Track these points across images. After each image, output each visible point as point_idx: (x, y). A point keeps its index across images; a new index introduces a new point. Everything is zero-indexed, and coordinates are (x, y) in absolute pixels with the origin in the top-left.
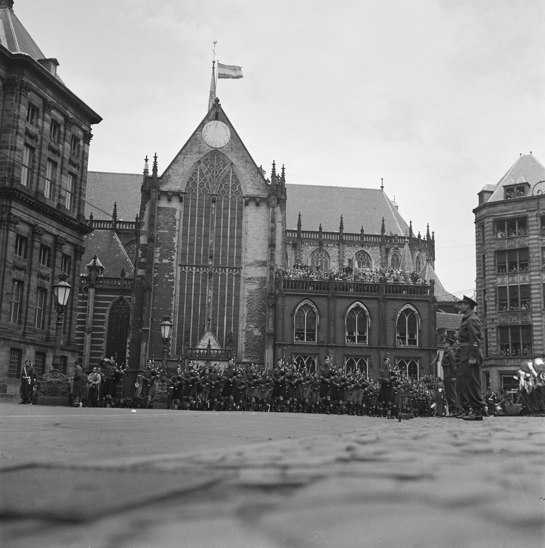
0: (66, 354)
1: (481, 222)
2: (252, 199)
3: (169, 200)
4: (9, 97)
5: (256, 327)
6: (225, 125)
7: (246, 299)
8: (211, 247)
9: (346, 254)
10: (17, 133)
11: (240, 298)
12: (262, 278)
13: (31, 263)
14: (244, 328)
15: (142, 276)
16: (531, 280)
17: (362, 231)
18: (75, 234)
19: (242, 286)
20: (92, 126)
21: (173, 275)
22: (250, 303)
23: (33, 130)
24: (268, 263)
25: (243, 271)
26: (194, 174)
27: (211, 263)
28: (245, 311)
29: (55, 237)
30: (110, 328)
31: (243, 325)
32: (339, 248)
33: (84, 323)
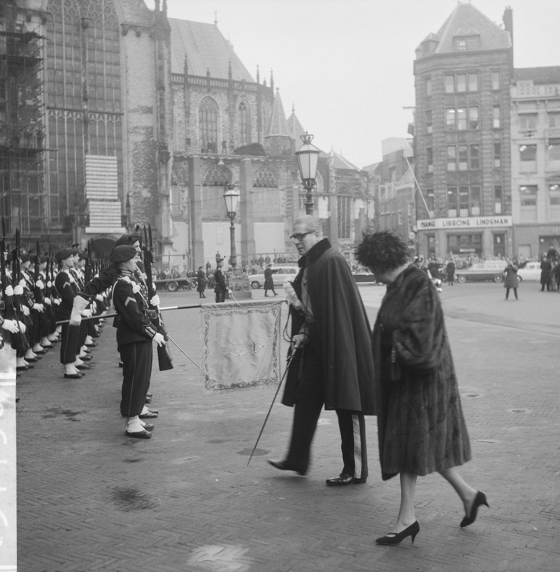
1: (428, 73)
2: (133, 27)
5: (145, 187)
7: (131, 153)
8: (85, 87)
9: (192, 99)
11: (123, 152)
12: (147, 128)
14: (131, 187)
16: (482, 140)
17: (208, 73)
19: (125, 137)
21: (41, 121)
25: (124, 118)
27: (85, 107)
28: (130, 167)
32: (184, 92)
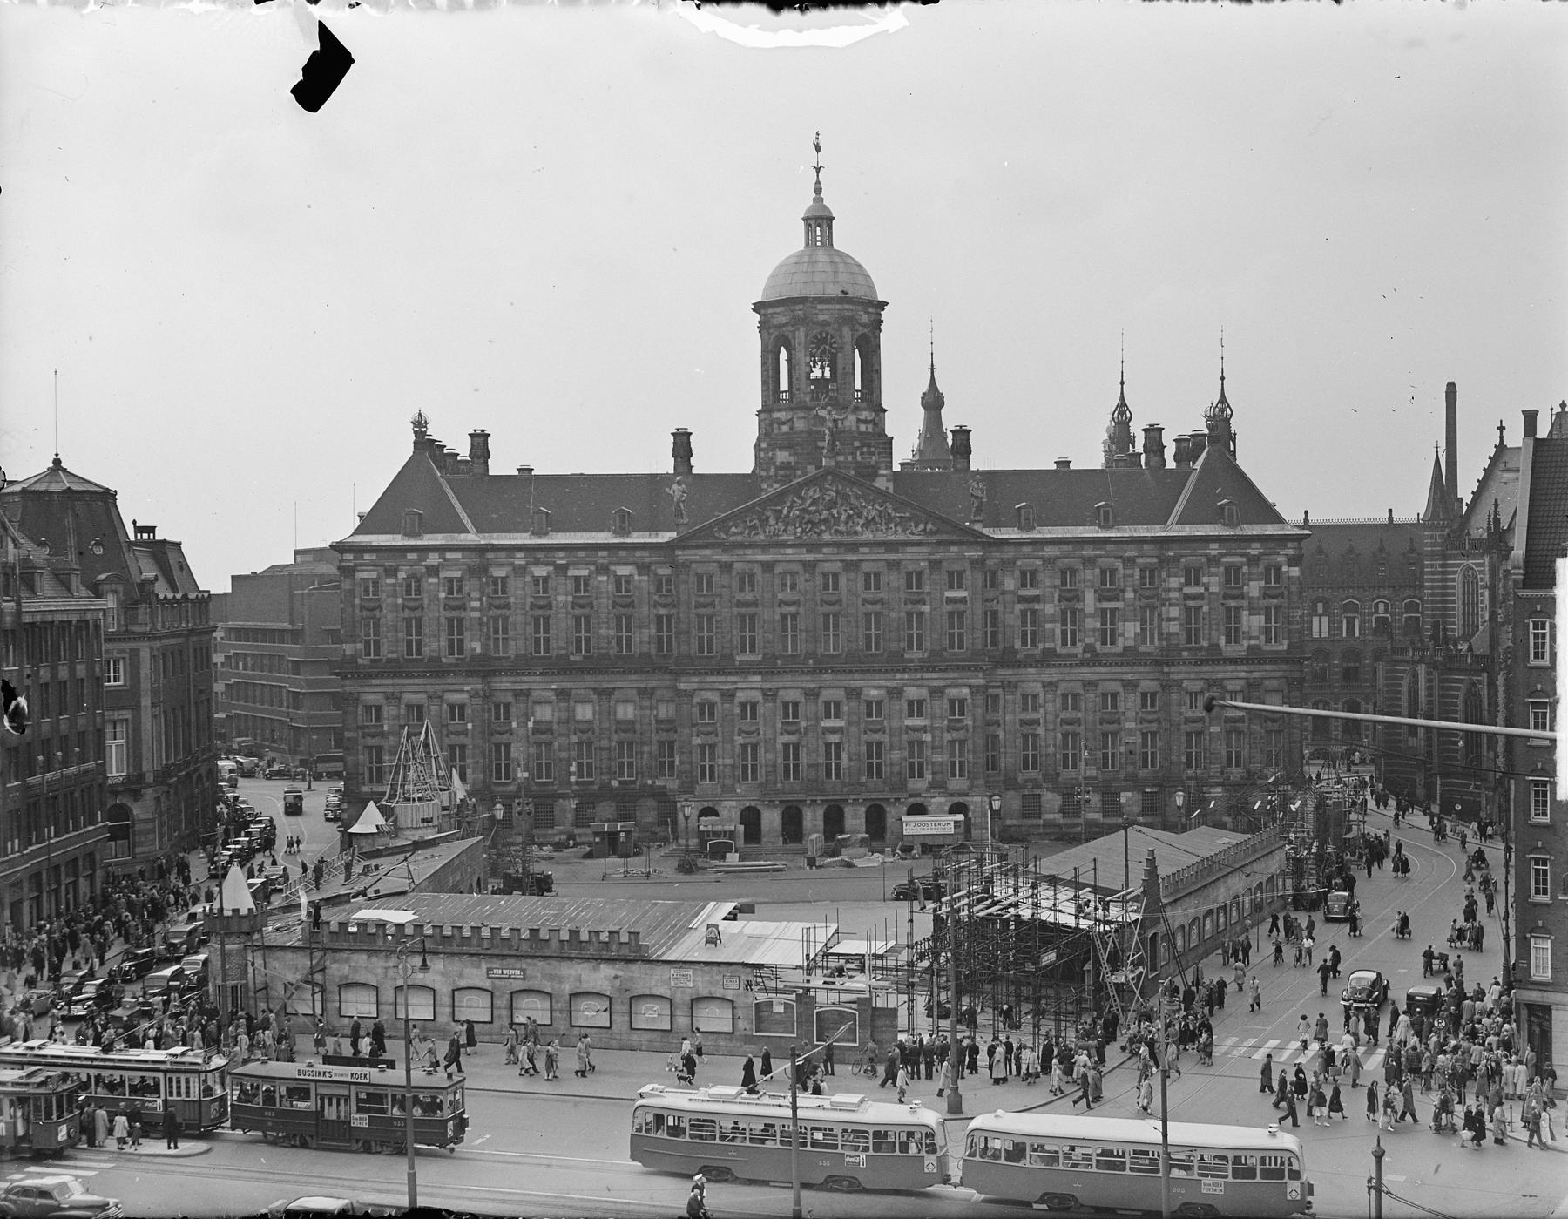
18: (1284, 667)
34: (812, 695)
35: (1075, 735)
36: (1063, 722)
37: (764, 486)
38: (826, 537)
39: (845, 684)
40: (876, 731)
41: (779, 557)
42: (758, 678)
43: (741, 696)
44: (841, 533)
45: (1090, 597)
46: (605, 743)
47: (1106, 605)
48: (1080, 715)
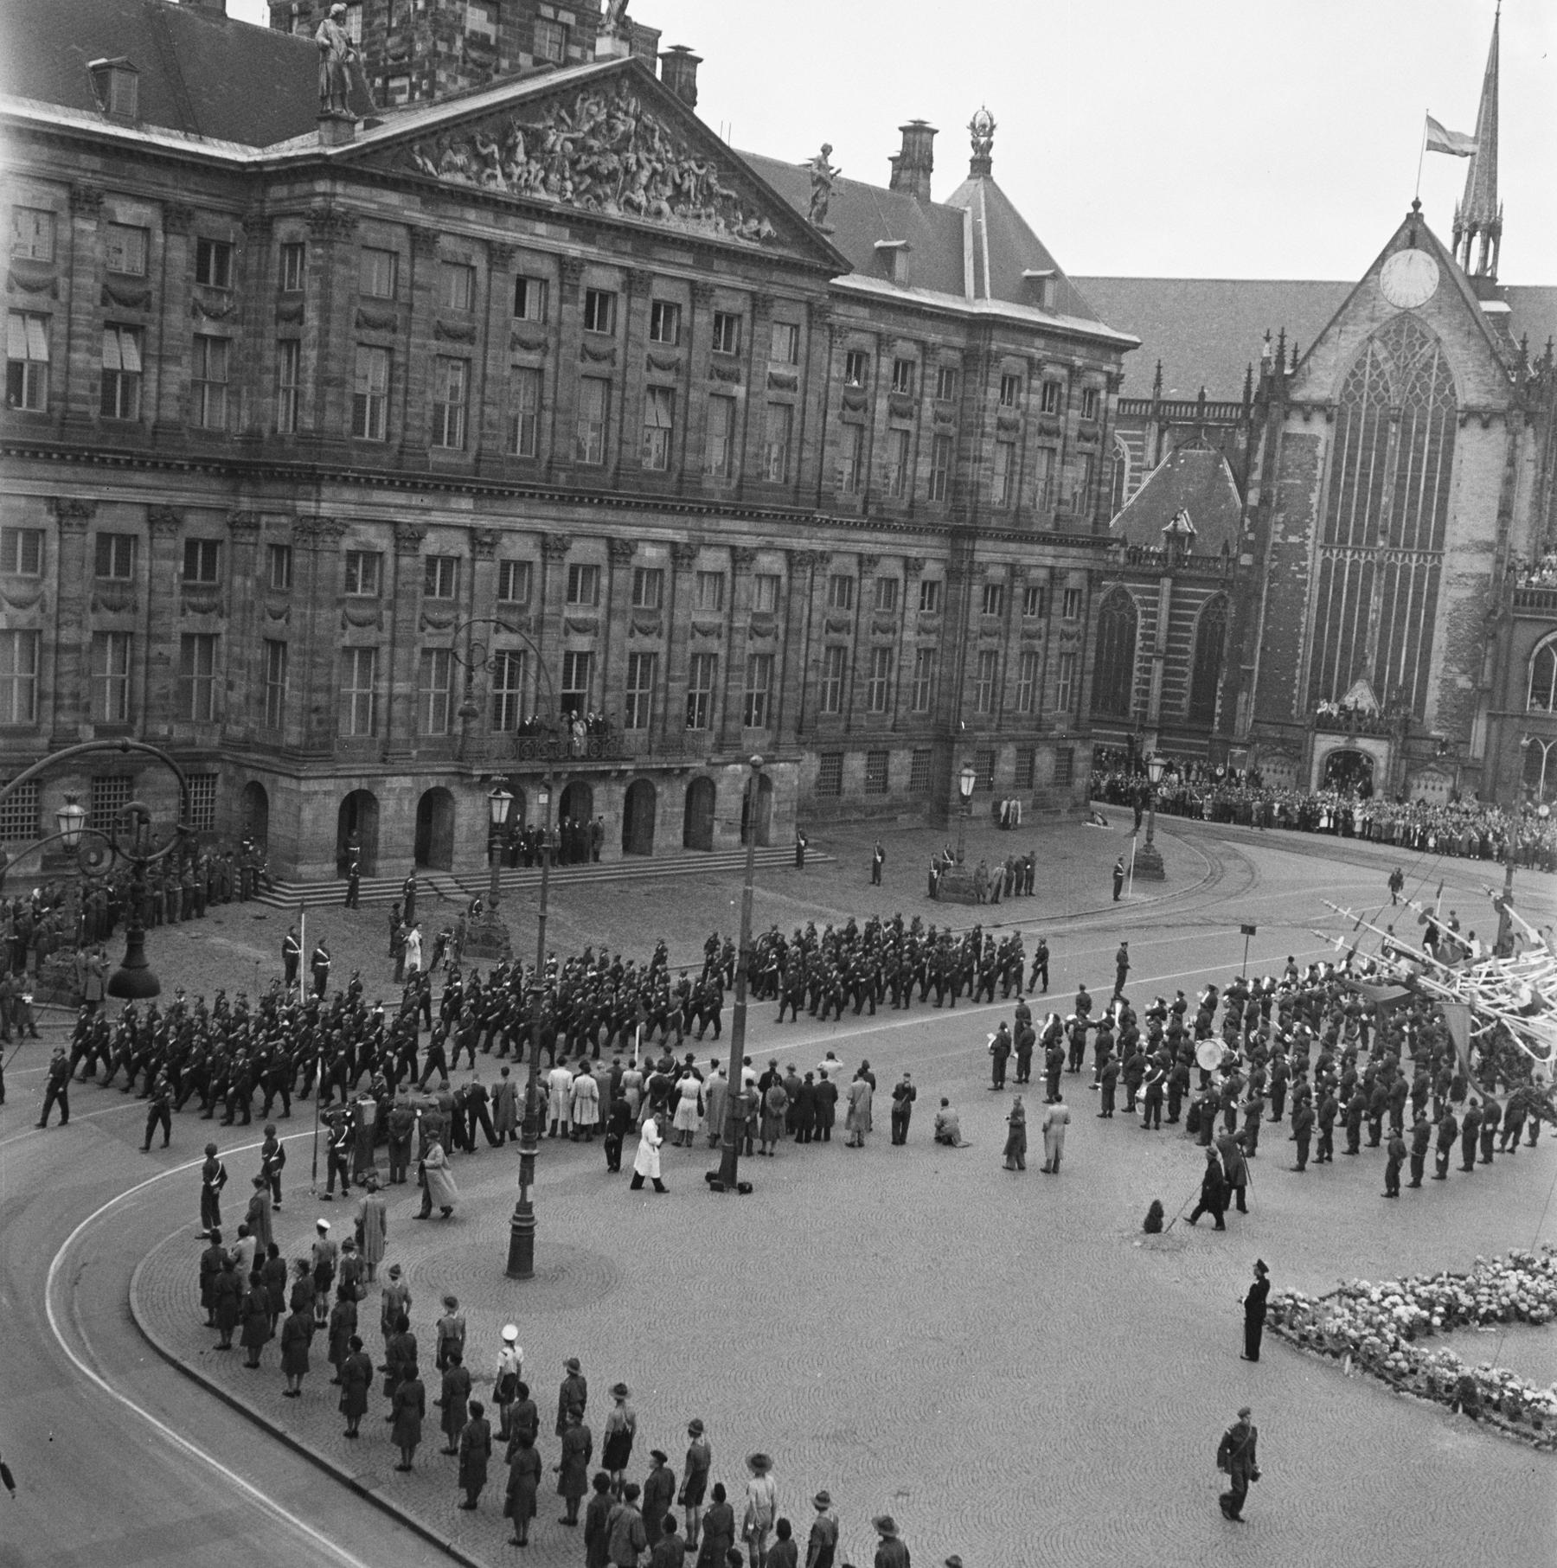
0: (1070, 744)
2: (1471, 413)
3: (1307, 419)
4: (970, 376)
5: (1464, 672)
6: (1428, 257)
10: (983, 435)
12: (1481, 576)
13: (1008, 622)
15: (1248, 568)
18: (1089, 552)
19: (1441, 589)
20: (1126, 358)
22: (1454, 624)
23: (1009, 414)
24: (1498, 547)
25: (1445, 560)
26: (1360, 364)
29: (1052, 568)
30: (1199, 650)
31: (1437, 665)
33: (1152, 637)
34: (552, 547)
35: (840, 649)
36: (833, 627)
37: (442, 77)
38: (613, 211)
39: (610, 530)
40: (646, 632)
41: (524, 239)
42: (466, 503)
43: (432, 544)
44: (637, 208)
45: (882, 405)
46: (68, 635)
47: (898, 423)
48: (851, 615)
